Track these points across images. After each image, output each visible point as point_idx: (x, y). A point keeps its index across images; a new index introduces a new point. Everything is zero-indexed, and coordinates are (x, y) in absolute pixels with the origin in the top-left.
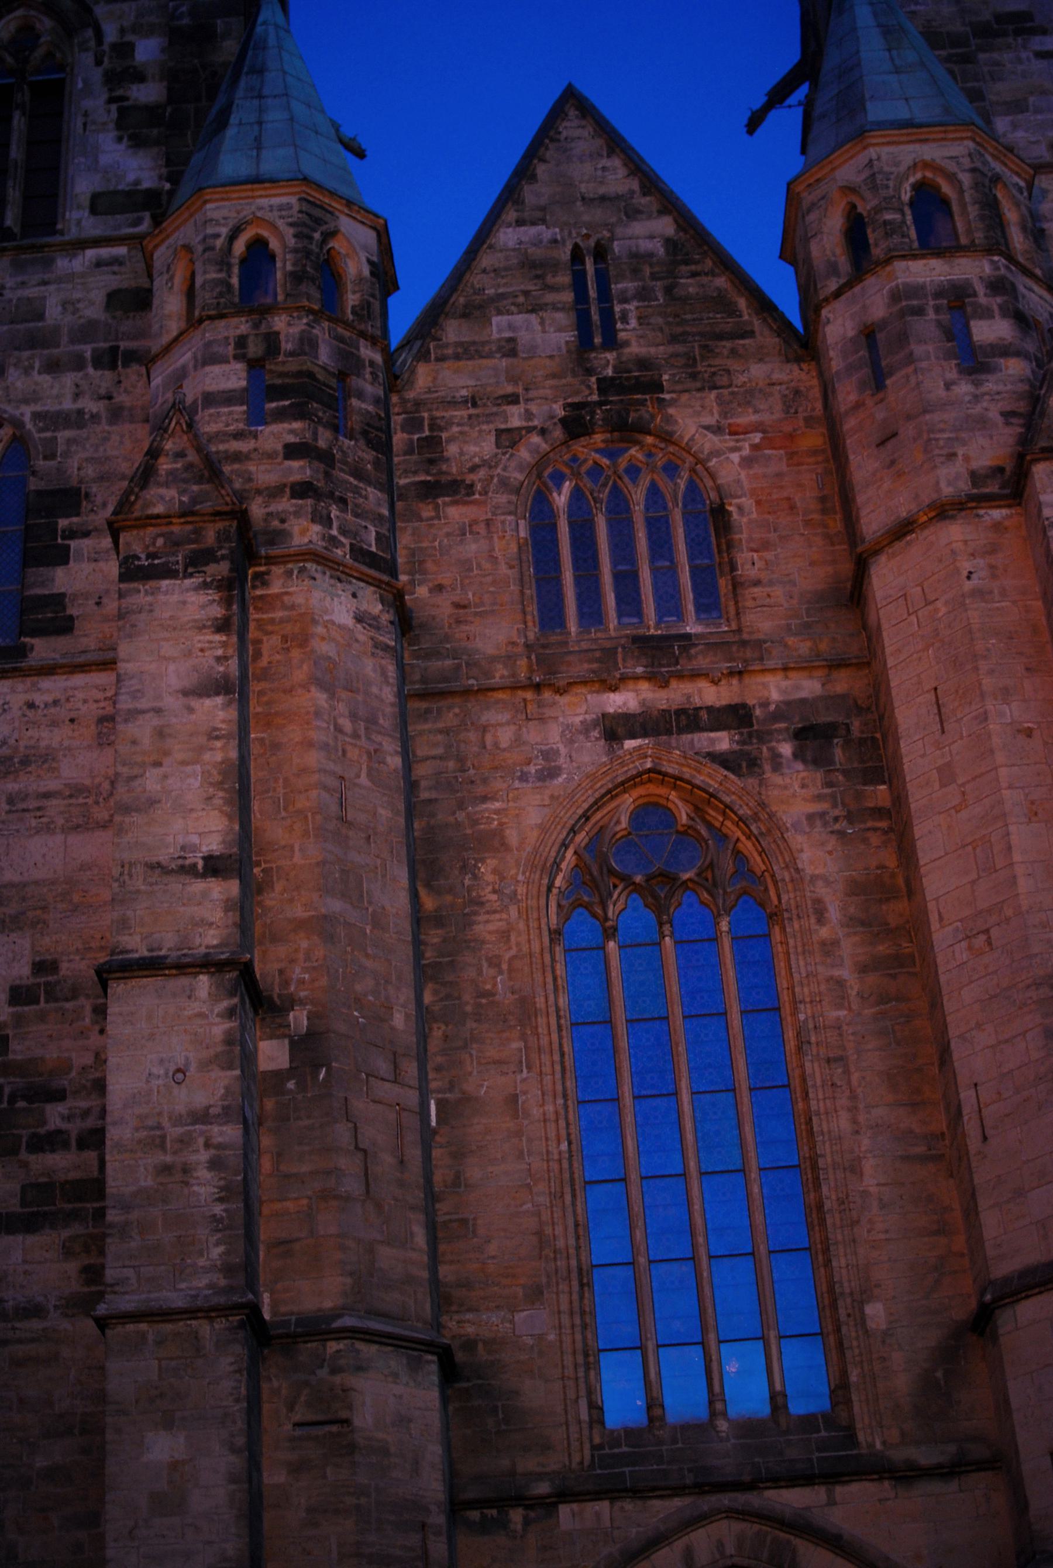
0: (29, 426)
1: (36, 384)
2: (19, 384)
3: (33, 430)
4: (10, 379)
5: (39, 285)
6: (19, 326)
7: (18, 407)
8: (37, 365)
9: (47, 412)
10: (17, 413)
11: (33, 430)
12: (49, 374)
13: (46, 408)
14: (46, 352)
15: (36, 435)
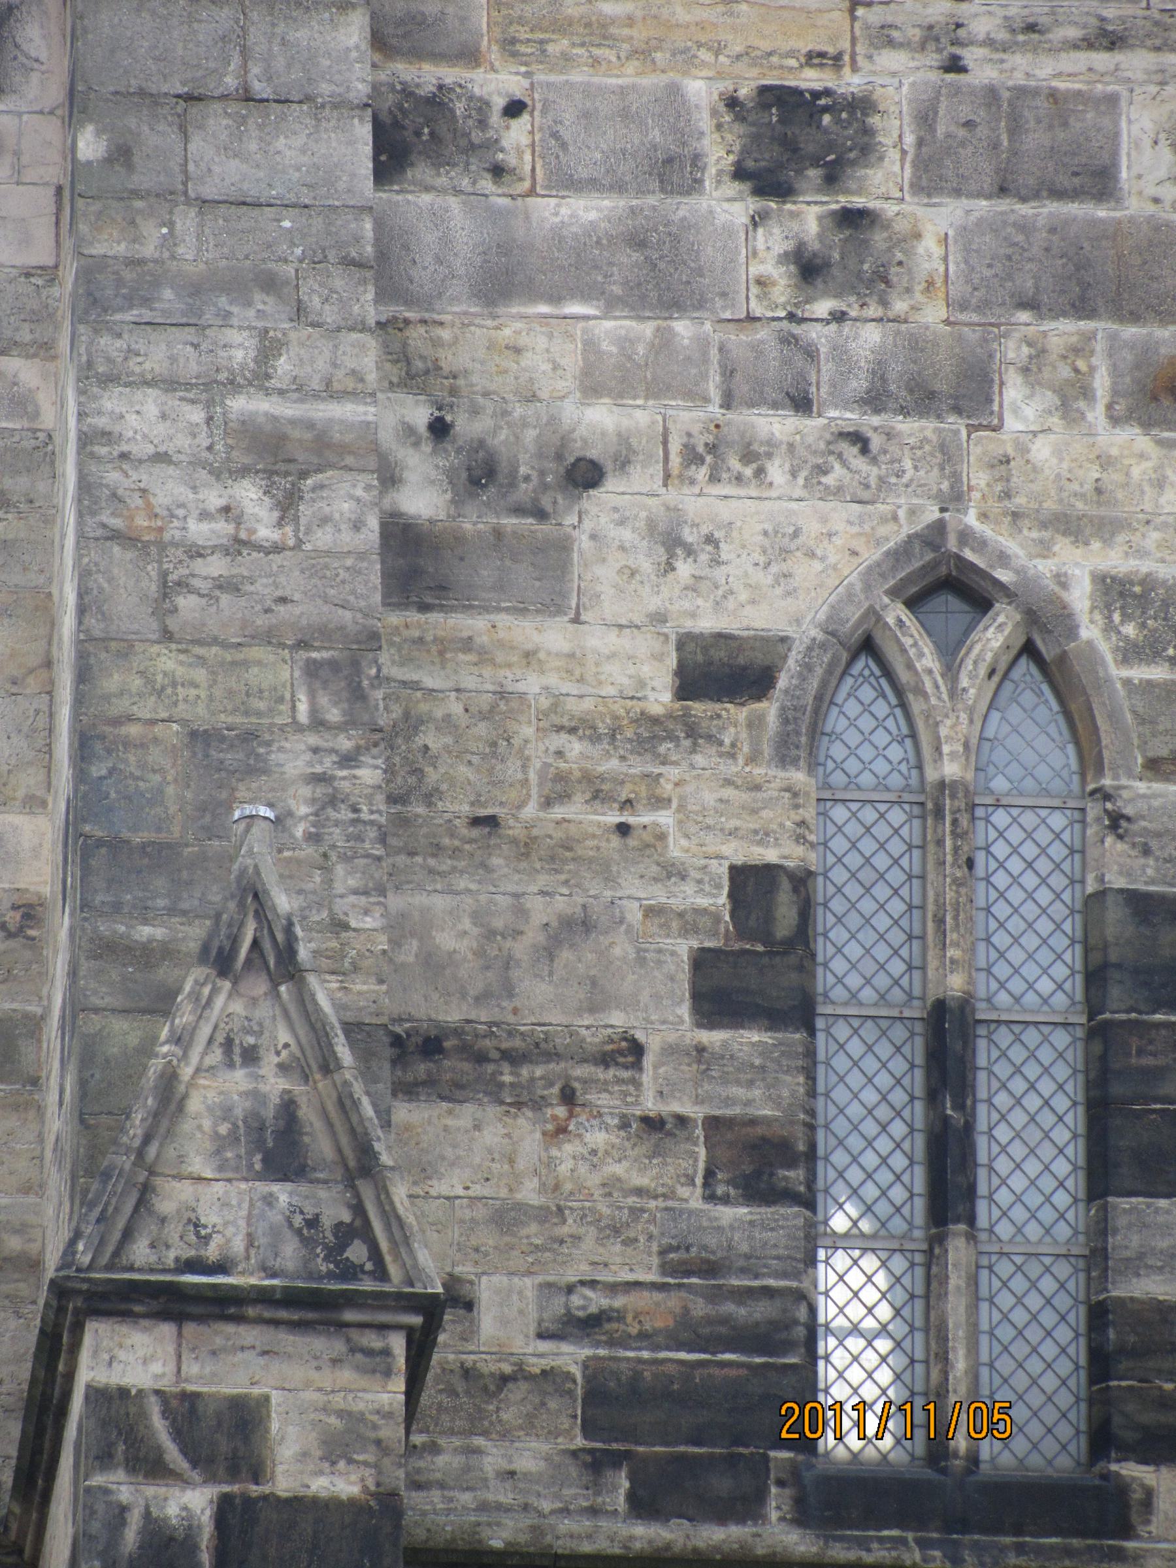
0: (1090, 631)
1: (1105, 461)
2: (1041, 450)
3: (1104, 648)
4: (1012, 424)
5: (1089, 44)
6: (1025, 210)
7: (1044, 549)
8: (1101, 383)
9: (1149, 582)
10: (1044, 567)
11: (1104, 648)
12: (1147, 425)
13: (1145, 567)
14: (1131, 332)
15: (1118, 672)
